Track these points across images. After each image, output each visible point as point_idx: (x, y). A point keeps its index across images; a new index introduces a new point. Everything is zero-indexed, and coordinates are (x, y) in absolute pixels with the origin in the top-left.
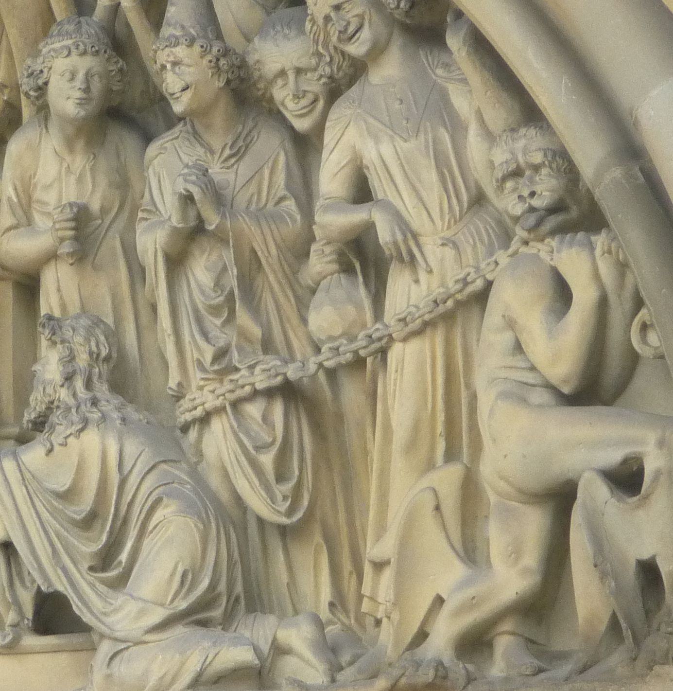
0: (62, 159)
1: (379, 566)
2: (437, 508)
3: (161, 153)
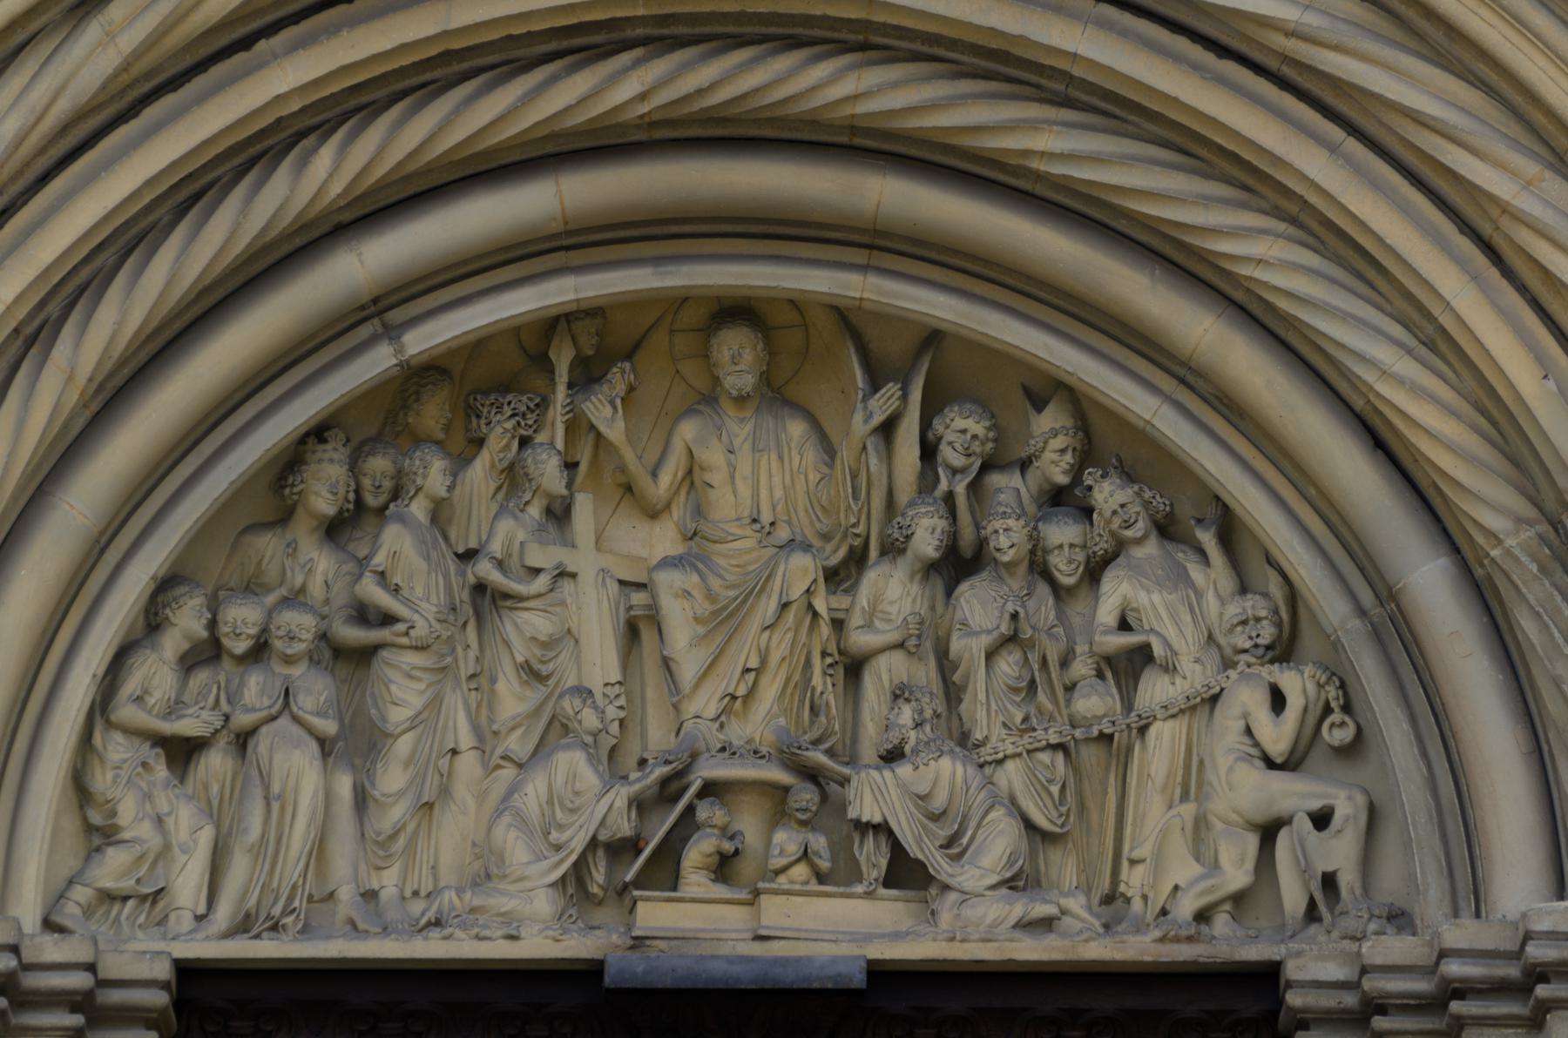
1: (1133, 862)
2: (1183, 829)
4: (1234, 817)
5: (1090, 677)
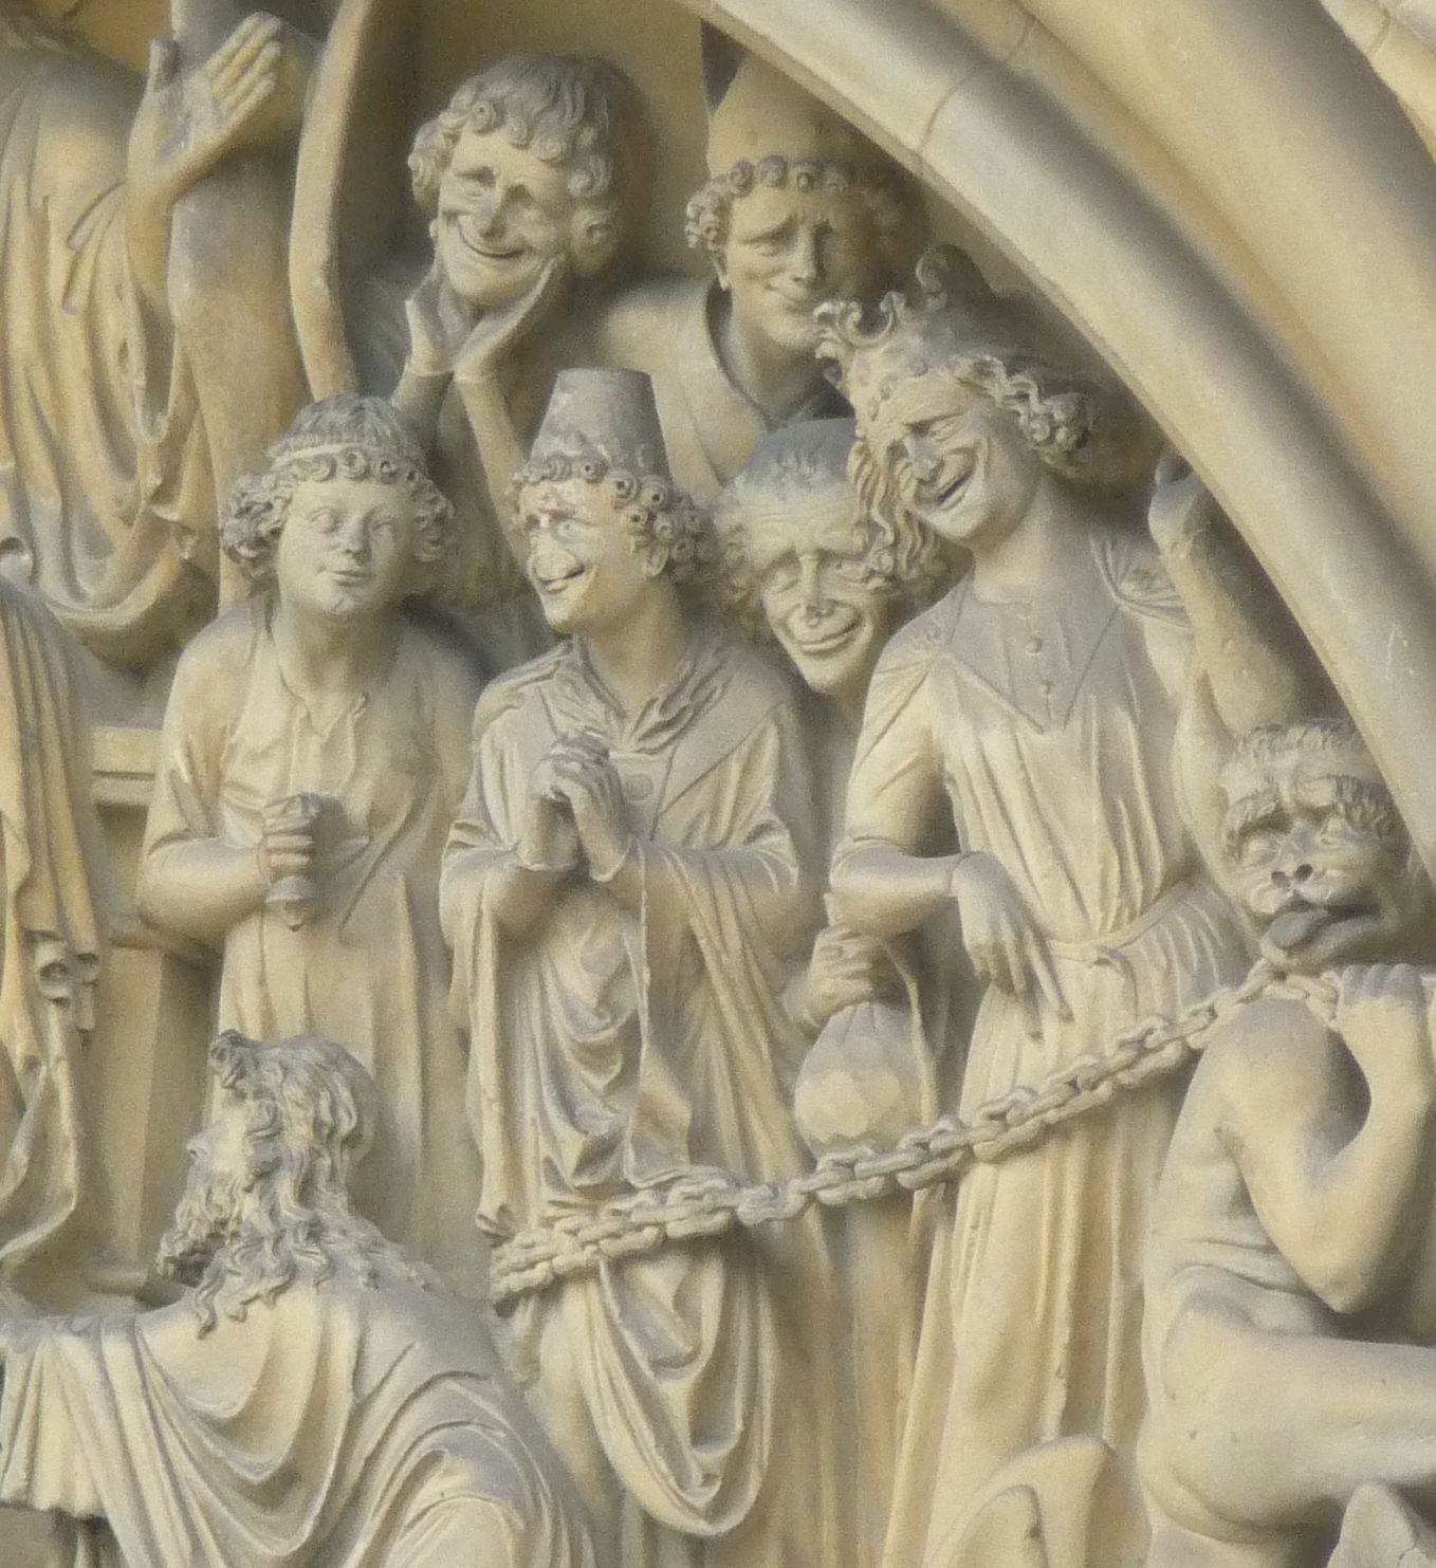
0: (296, 700)
2: (1036, 1532)
3: (511, 707)
4: (1180, 1493)
5: (856, 1002)
